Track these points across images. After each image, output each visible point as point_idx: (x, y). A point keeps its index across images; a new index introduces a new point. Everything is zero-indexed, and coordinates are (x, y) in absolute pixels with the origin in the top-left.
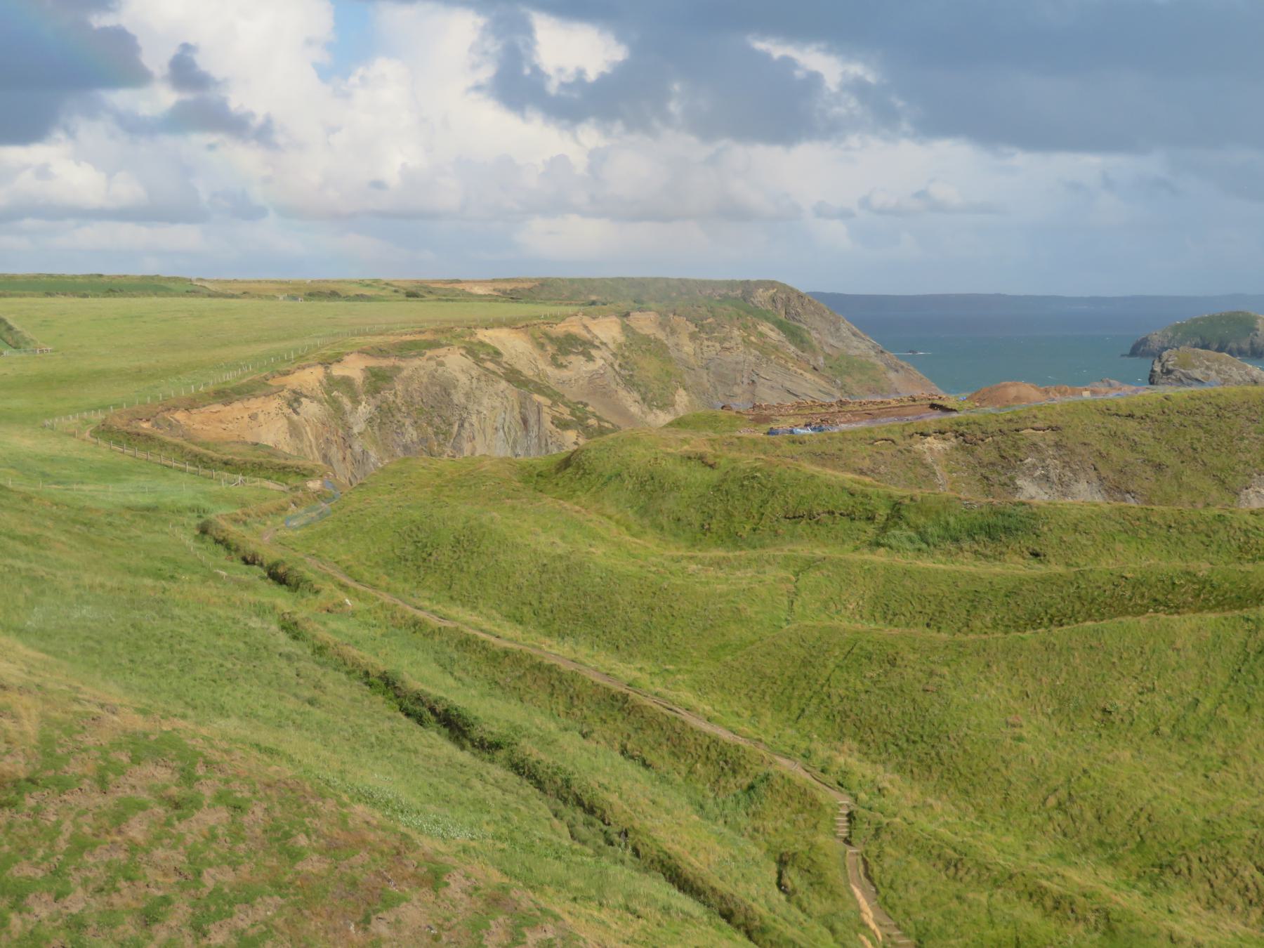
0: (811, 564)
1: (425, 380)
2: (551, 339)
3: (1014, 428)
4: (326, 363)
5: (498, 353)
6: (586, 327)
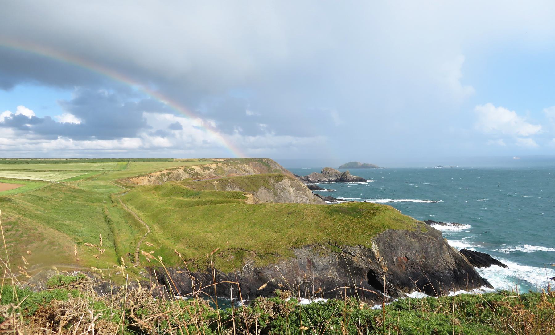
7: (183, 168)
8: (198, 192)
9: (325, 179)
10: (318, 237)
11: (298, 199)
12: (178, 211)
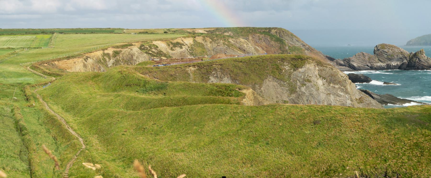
0: (119, 96)
1: (127, 54)
2: (172, 43)
3: (210, 65)
4: (103, 50)
5: (157, 47)
6: (182, 40)
7: (138, 45)
8: (162, 84)
9: (379, 64)
10: (365, 165)
11: (332, 97)
12: (130, 115)
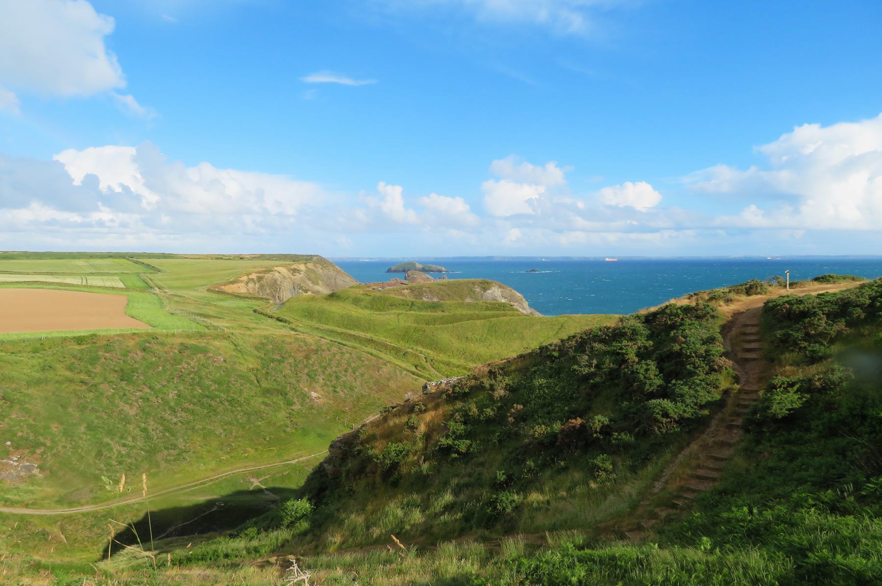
0: (399, 314)
